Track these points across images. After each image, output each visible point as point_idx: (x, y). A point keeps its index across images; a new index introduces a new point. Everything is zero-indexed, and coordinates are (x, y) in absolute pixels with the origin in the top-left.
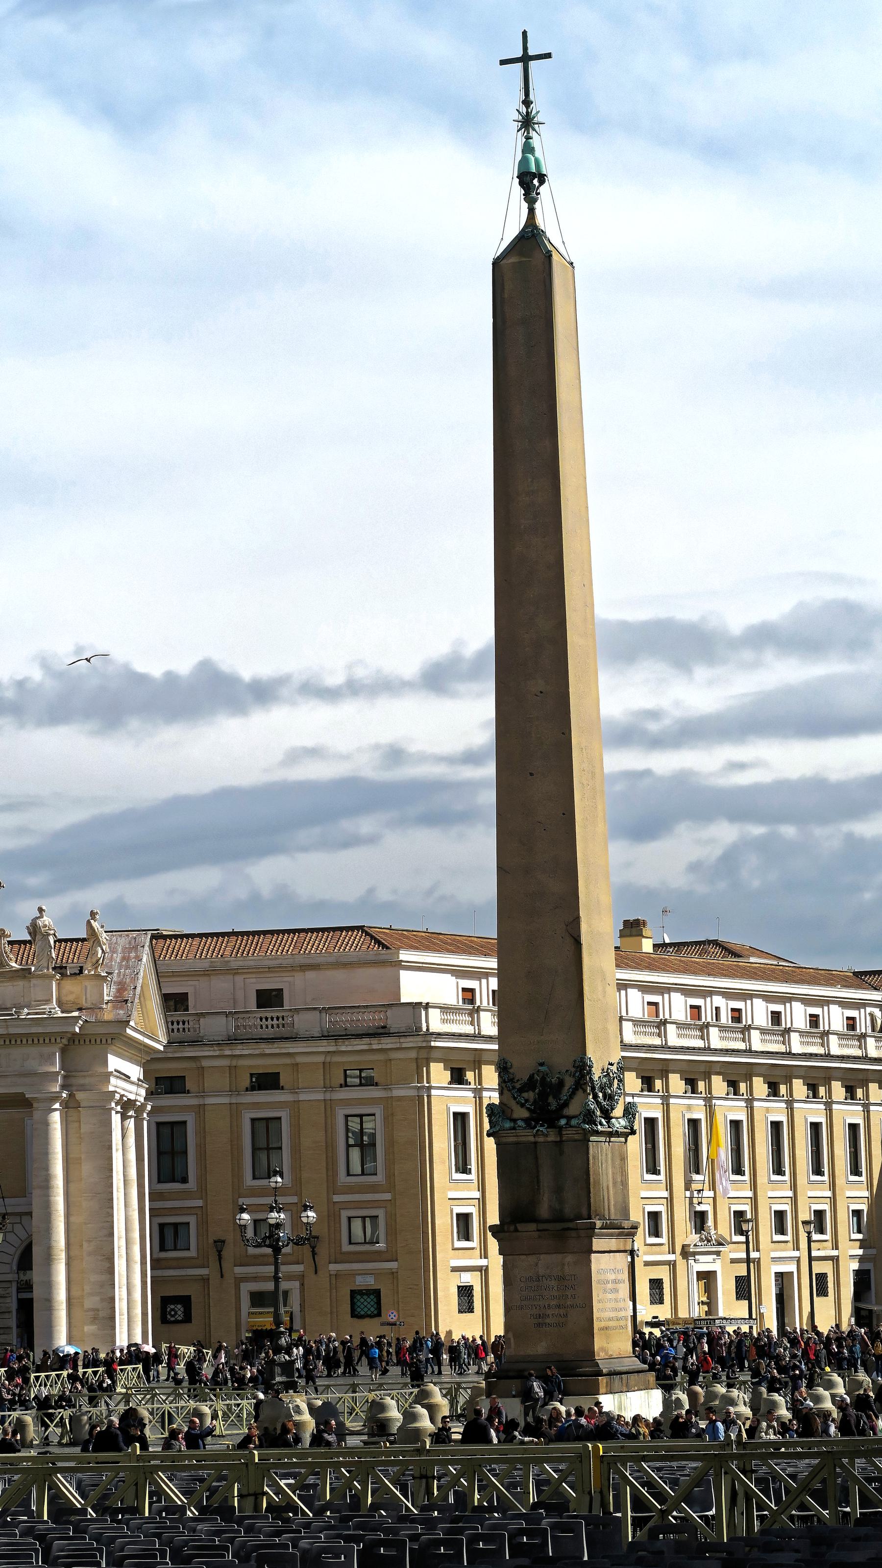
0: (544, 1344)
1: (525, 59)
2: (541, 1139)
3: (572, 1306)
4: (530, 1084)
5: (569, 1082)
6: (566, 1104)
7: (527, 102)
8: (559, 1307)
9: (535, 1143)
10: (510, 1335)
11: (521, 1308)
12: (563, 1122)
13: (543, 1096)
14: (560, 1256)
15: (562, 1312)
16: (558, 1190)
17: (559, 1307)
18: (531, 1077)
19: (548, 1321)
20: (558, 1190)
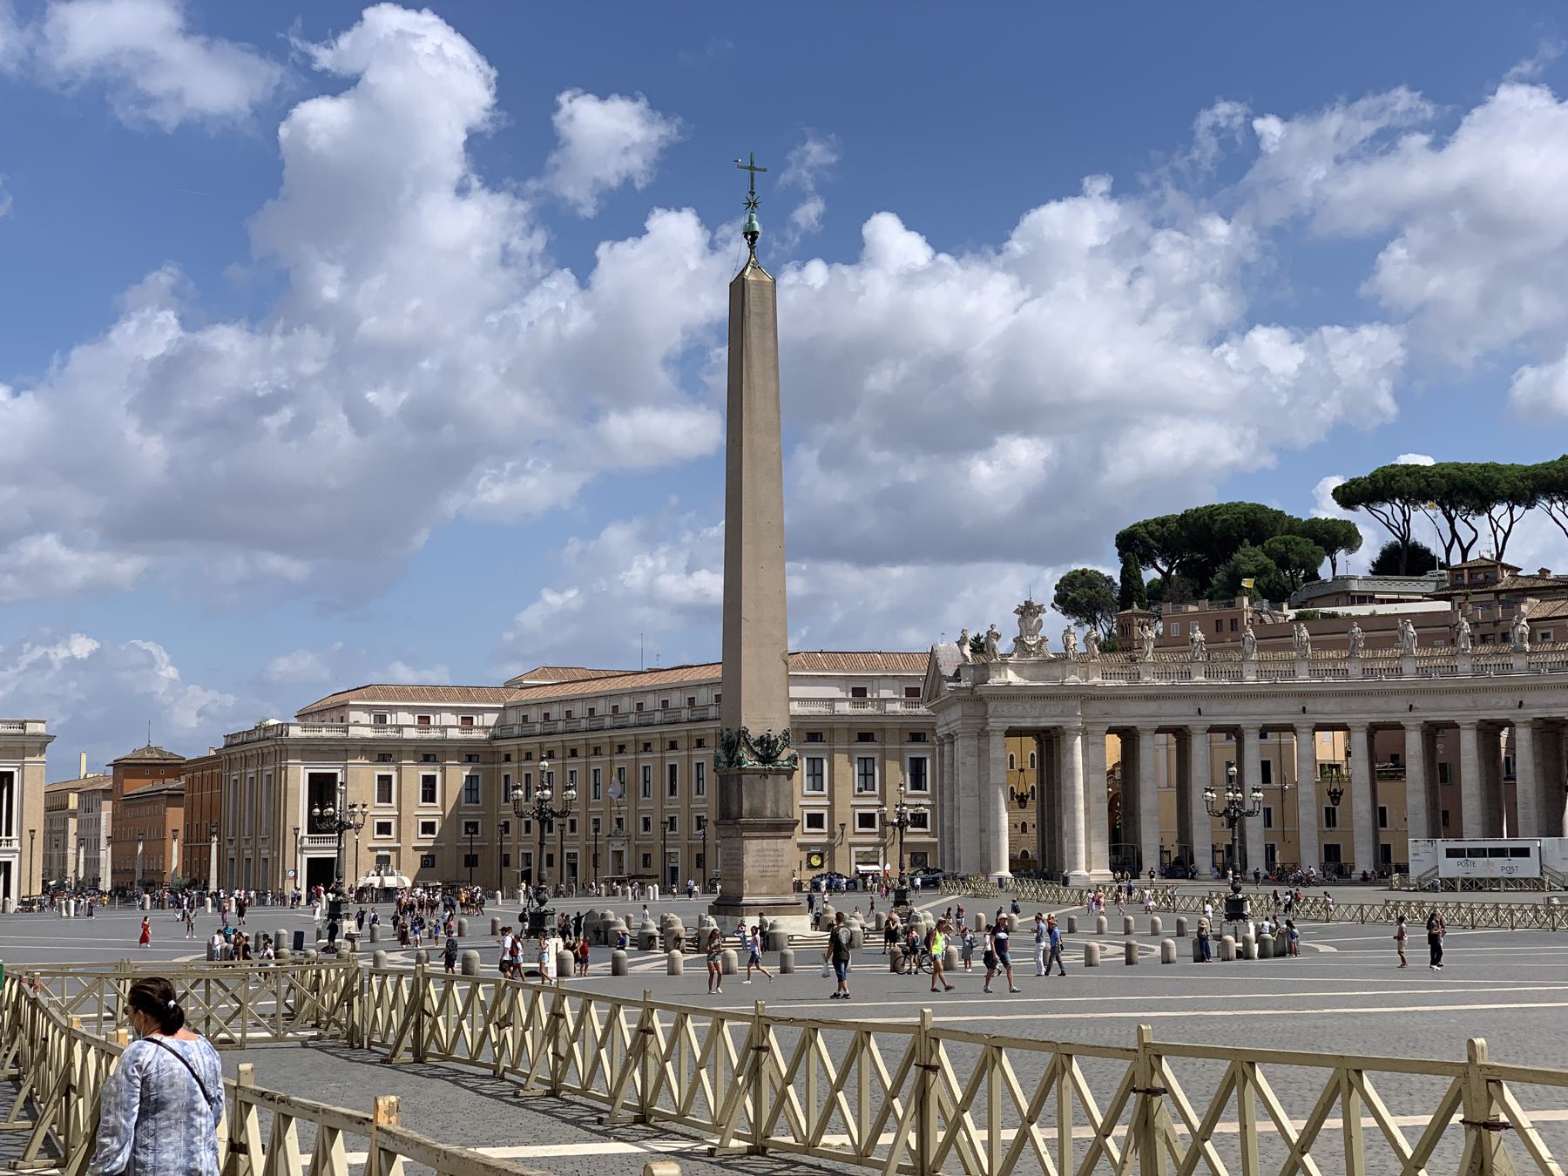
1: (752, 168)
4: (761, 741)
7: (752, 193)
16: (776, 802)
20: (776, 802)
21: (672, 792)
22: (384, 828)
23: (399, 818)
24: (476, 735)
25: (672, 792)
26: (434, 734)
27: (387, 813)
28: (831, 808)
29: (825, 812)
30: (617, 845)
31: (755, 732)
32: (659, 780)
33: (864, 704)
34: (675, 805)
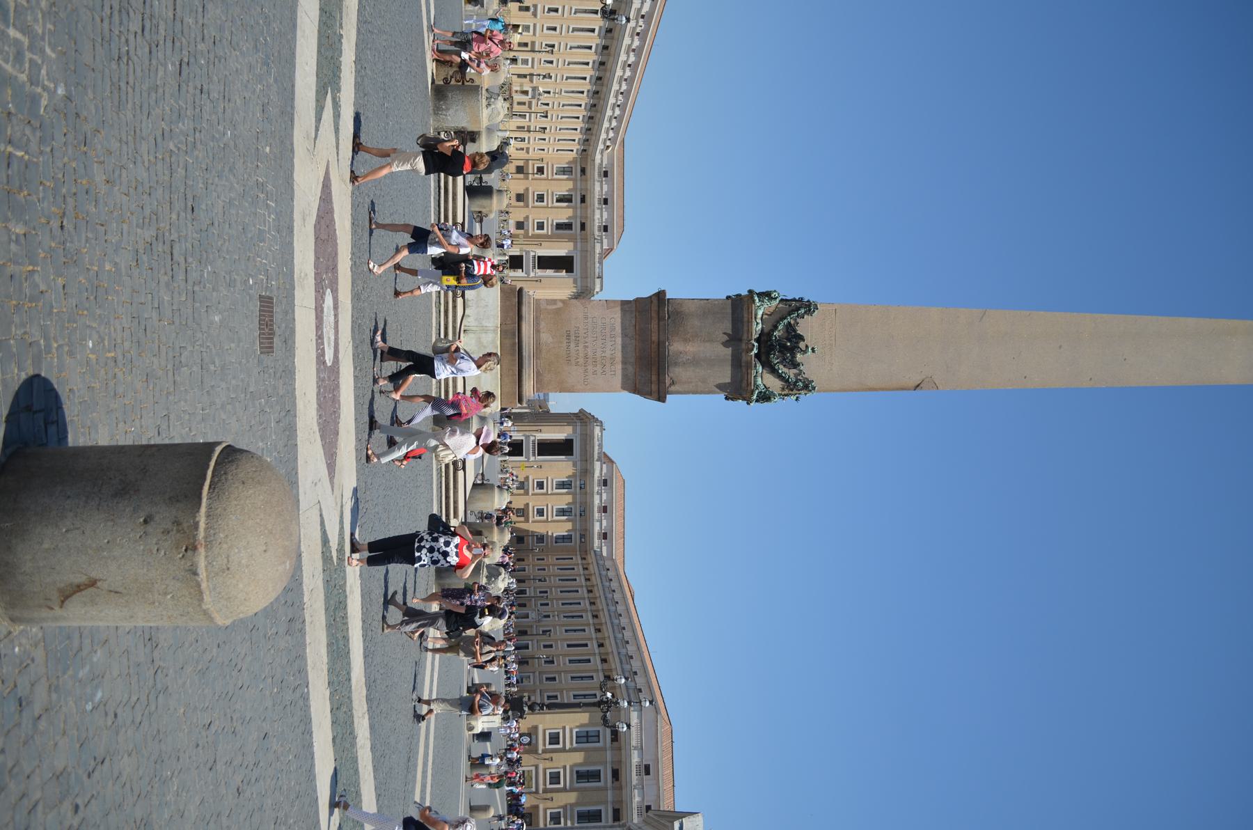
0: (550, 340)
2: (744, 346)
3: (586, 371)
4: (794, 337)
5: (791, 373)
6: (773, 371)
8: (586, 357)
9: (740, 340)
10: (560, 305)
11: (586, 318)
12: (760, 369)
13: (783, 349)
14: (633, 360)
15: (581, 360)
16: (695, 362)
17: (586, 357)
18: (801, 338)
19: (572, 345)
20: (695, 362)
21: (569, 646)
22: (540, 485)
23: (547, 494)
24: (596, 542)
25: (569, 646)
26: (596, 515)
27: (550, 487)
28: (564, 750)
29: (561, 746)
30: (533, 615)
31: (807, 326)
32: (576, 637)
33: (639, 774)
34: (561, 647)
